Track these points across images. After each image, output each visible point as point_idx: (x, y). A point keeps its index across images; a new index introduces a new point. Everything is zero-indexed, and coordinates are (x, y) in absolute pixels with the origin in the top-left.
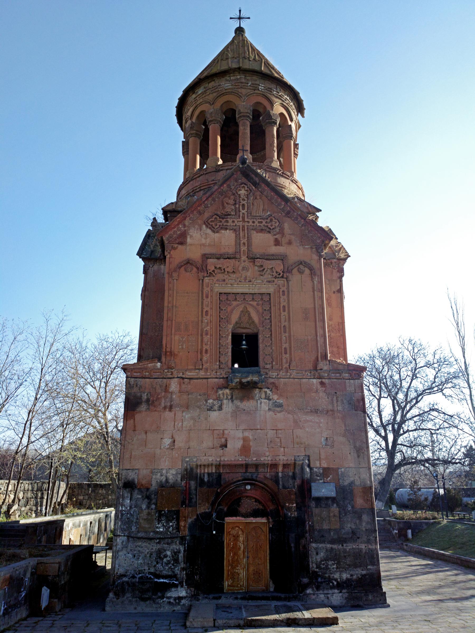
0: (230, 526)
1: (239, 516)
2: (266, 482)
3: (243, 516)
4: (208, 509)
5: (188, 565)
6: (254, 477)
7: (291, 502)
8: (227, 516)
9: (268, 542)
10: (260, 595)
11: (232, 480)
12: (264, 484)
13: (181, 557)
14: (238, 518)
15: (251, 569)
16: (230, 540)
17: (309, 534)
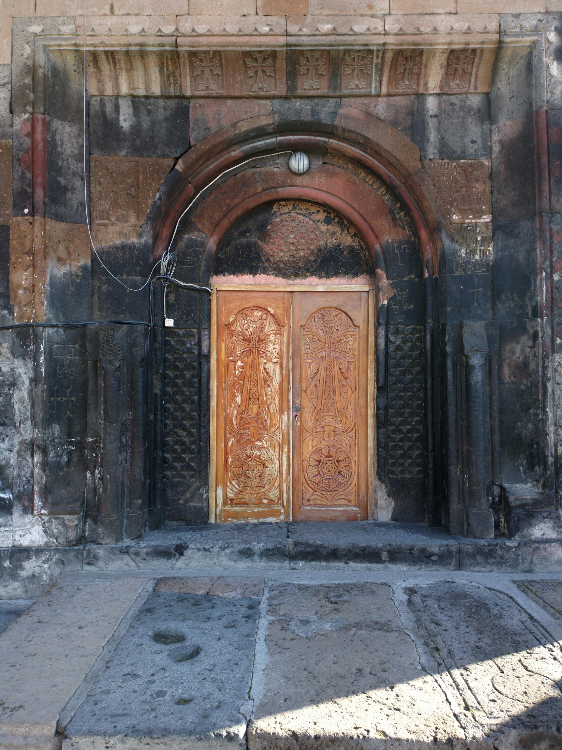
0: (232, 305)
1: (265, 271)
2: (370, 134)
3: (281, 270)
4: (140, 236)
5: (56, 429)
6: (324, 117)
7: (470, 206)
8: (219, 271)
9: (371, 357)
10: (342, 541)
11: (234, 125)
12: (365, 144)
13: (22, 401)
14: (261, 278)
15: (309, 447)
16: (231, 351)
17: (551, 322)
